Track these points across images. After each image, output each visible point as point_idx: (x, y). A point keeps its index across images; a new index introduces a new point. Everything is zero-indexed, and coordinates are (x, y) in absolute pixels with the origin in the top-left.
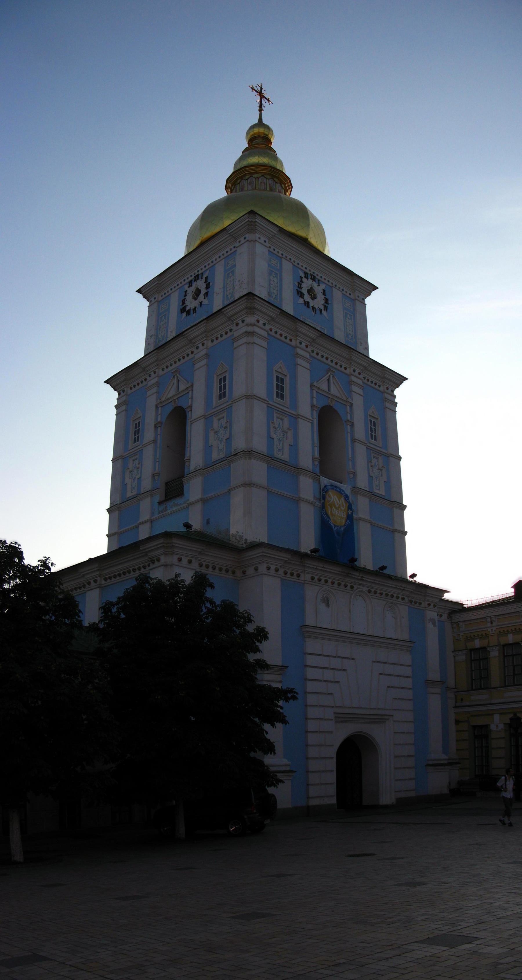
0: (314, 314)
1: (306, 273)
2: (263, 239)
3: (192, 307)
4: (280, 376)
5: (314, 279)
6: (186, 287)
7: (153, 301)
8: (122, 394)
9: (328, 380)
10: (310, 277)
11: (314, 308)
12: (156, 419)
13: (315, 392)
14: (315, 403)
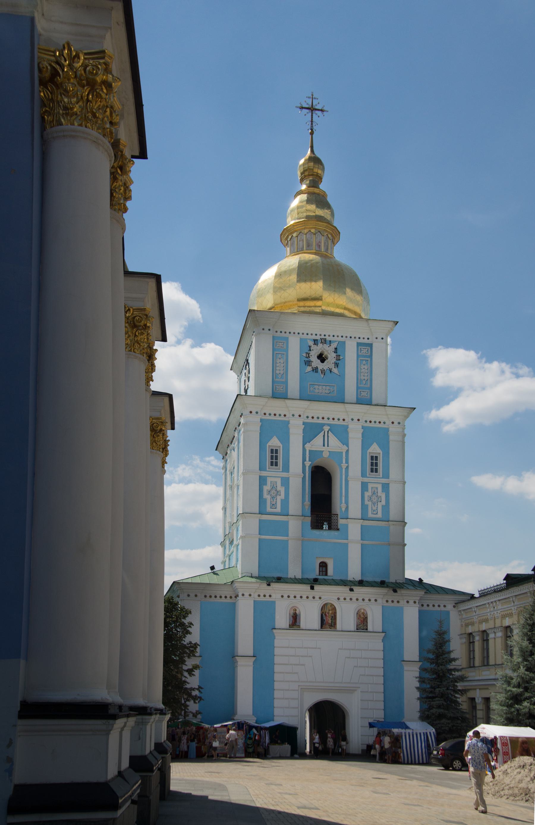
0: (322, 376)
5: (324, 341)
9: (324, 436)
11: (323, 371)
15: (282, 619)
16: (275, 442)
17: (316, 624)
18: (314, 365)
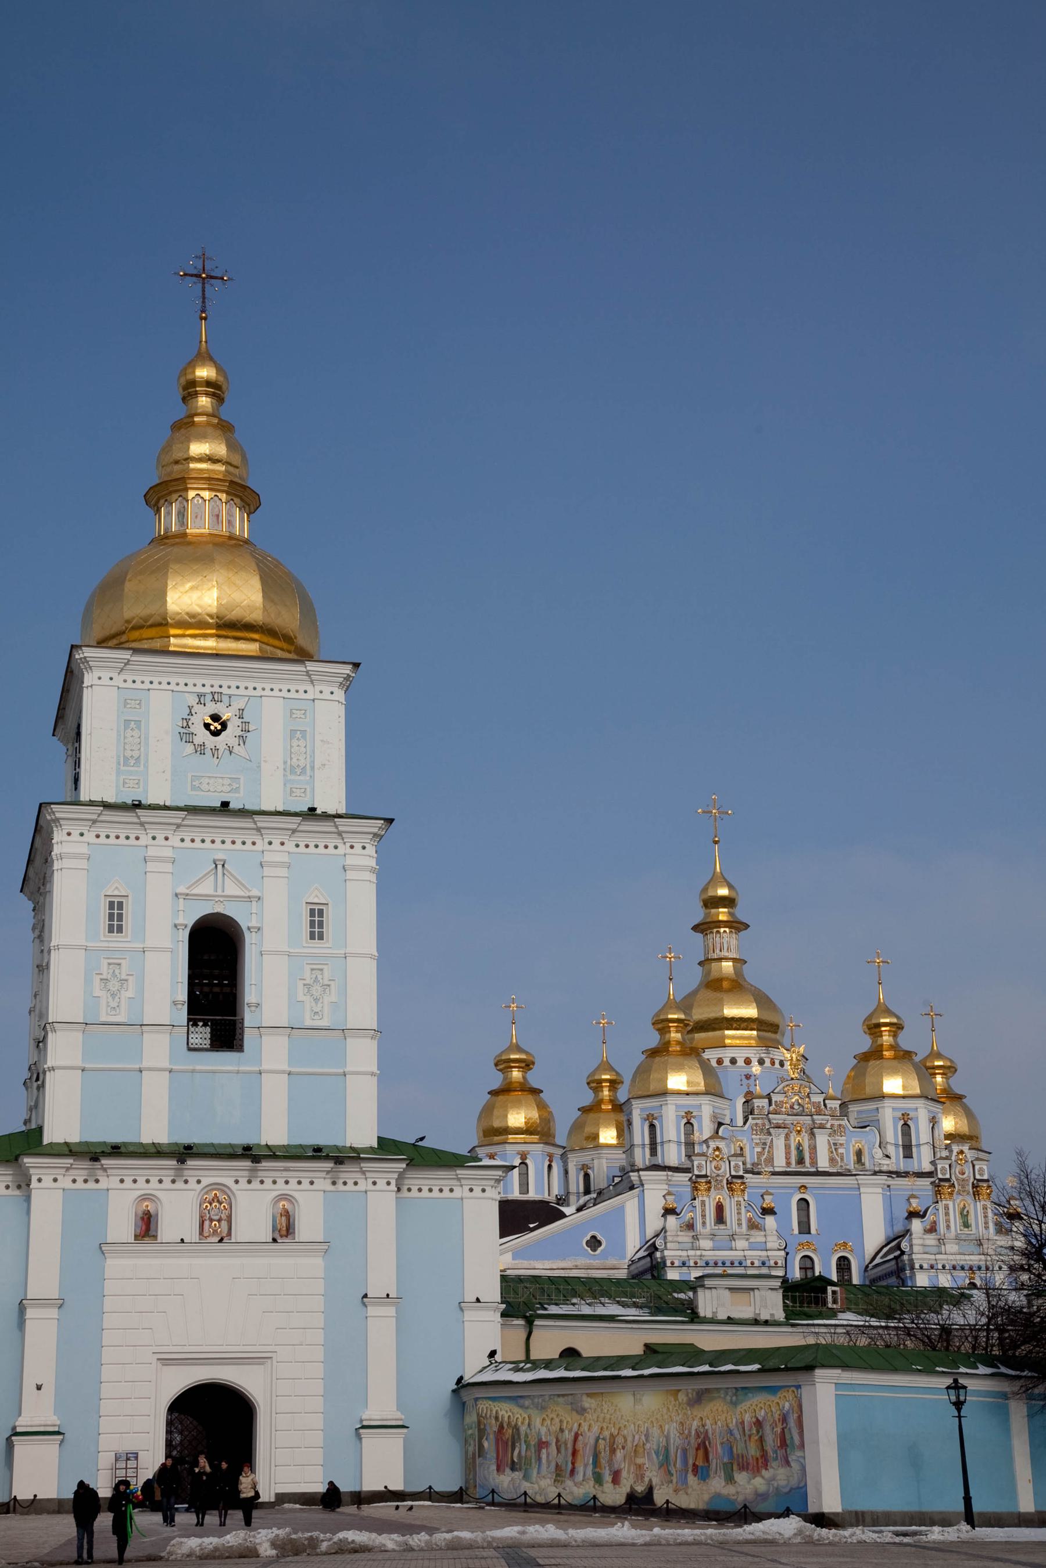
0: (216, 761)
1: (200, 696)
2: (105, 675)
4: (116, 900)
10: (209, 697)
13: (181, 900)
14: (181, 920)
15: (121, 1225)
16: (115, 888)
17: (191, 1233)
18: (197, 740)
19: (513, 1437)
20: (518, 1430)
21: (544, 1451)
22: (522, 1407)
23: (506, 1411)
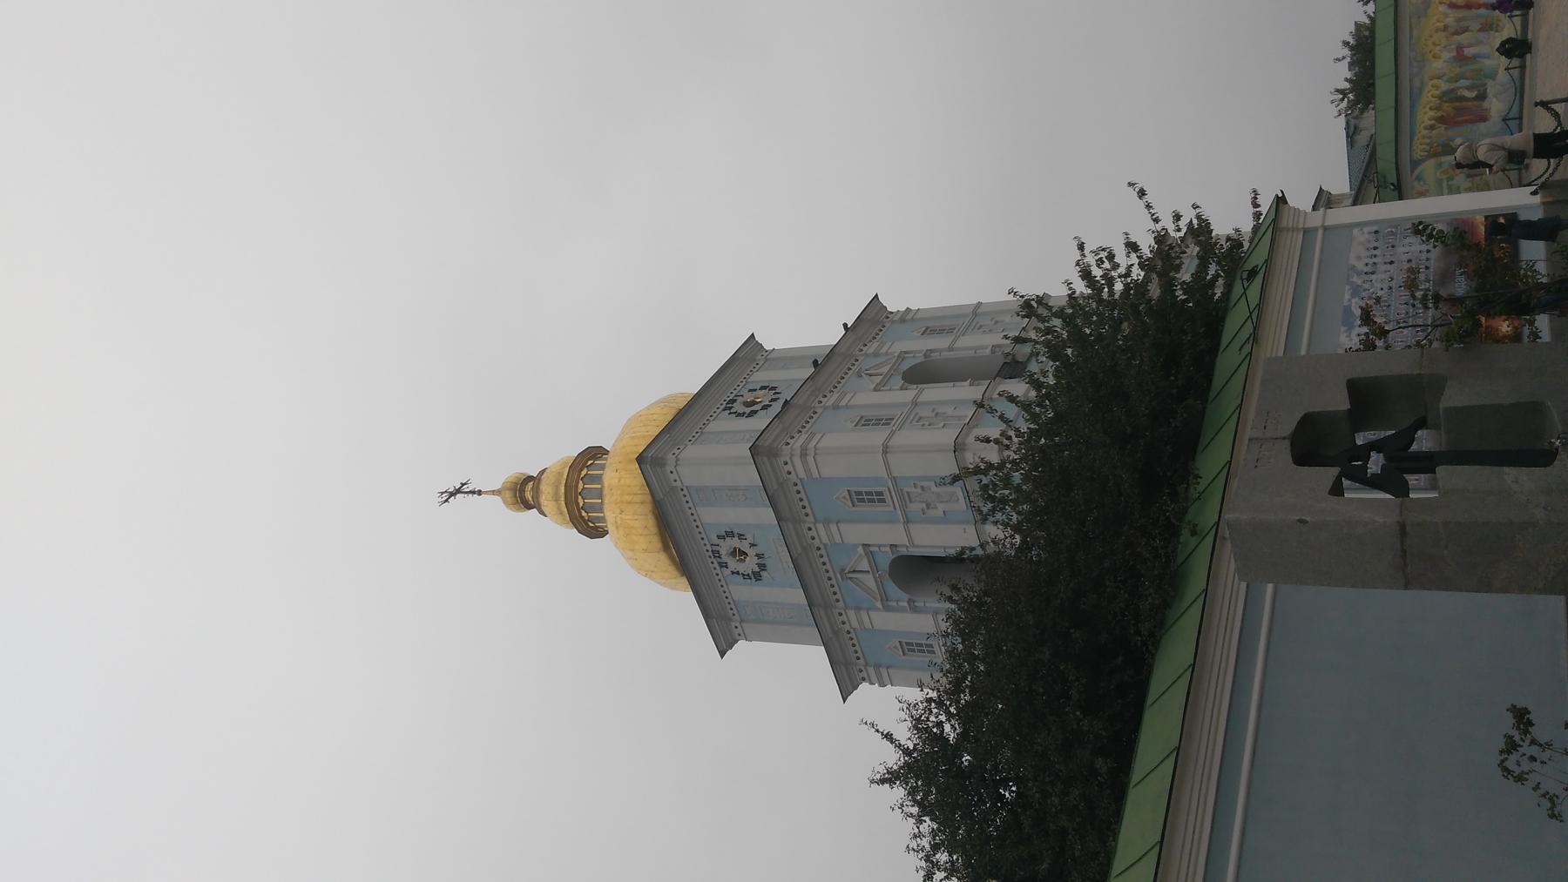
3: (756, 560)
6: (727, 572)
7: (739, 630)
8: (864, 674)
12: (902, 610)
19: (1451, 101)
20: (1444, 93)
21: (1468, 52)
22: (1421, 90)
23: (1425, 116)
